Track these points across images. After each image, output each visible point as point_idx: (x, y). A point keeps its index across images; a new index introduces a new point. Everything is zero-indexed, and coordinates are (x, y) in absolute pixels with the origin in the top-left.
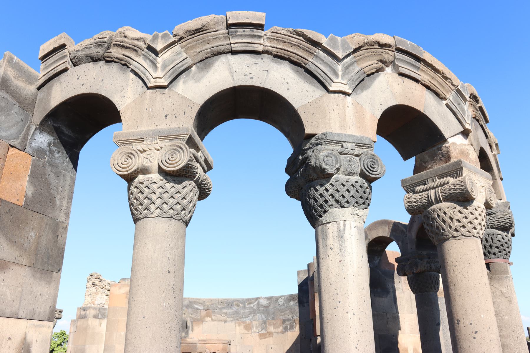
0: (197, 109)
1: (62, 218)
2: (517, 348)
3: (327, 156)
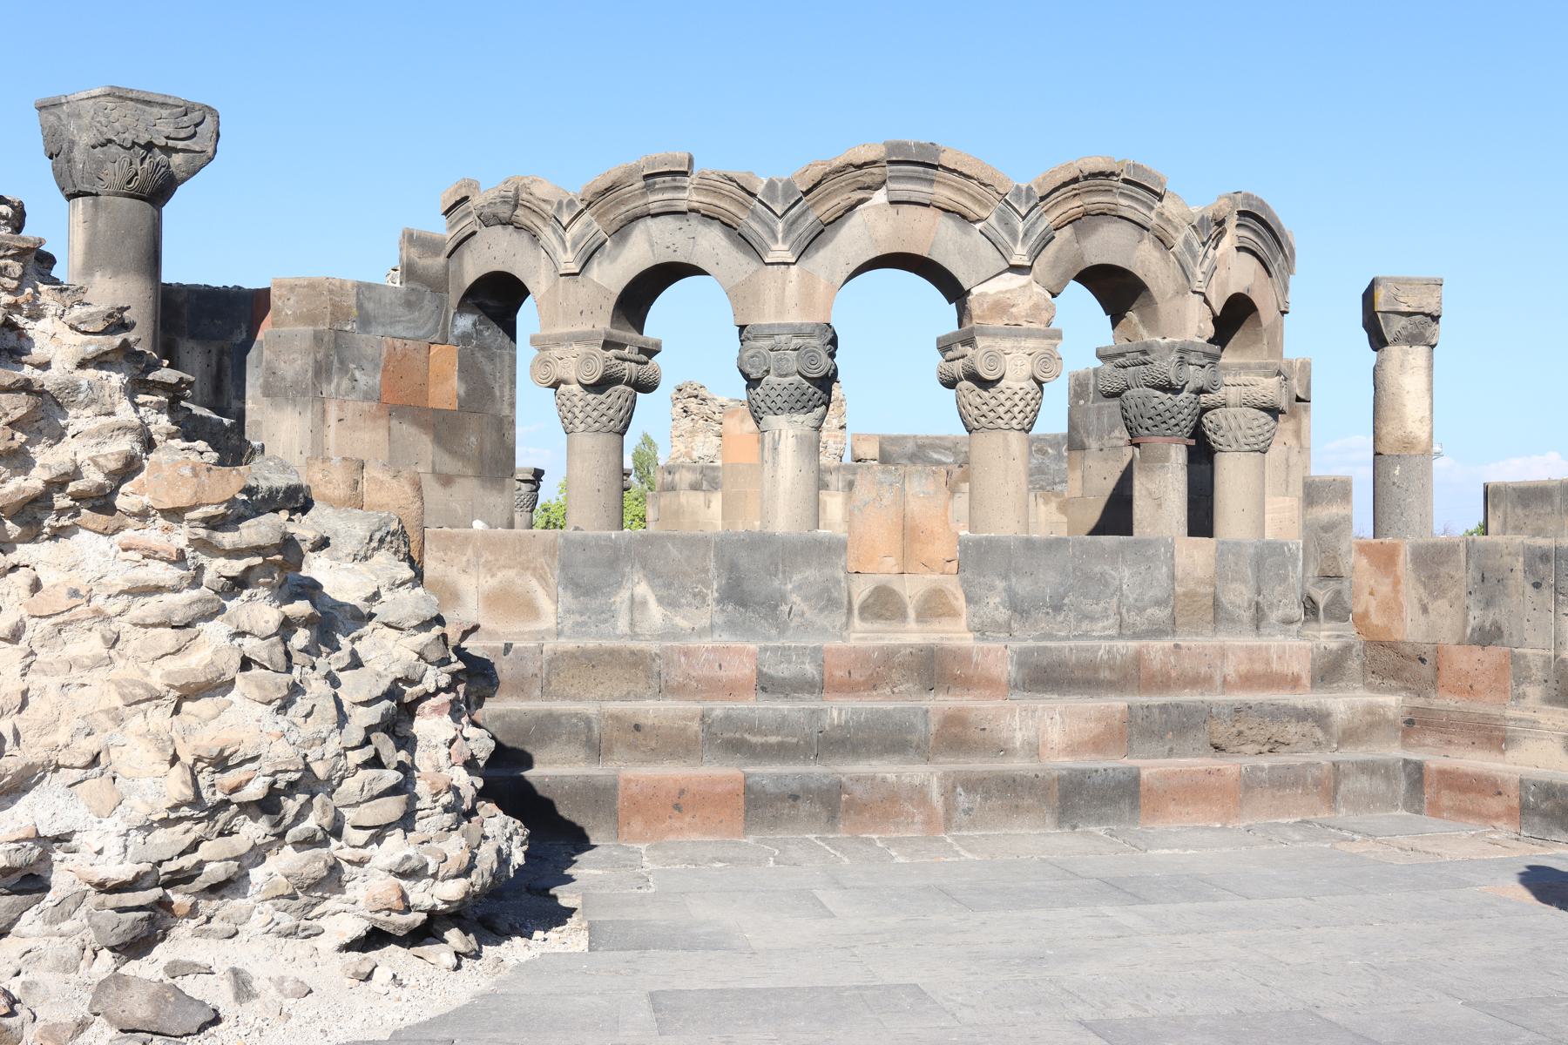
1: (506, 411)
3: (752, 357)
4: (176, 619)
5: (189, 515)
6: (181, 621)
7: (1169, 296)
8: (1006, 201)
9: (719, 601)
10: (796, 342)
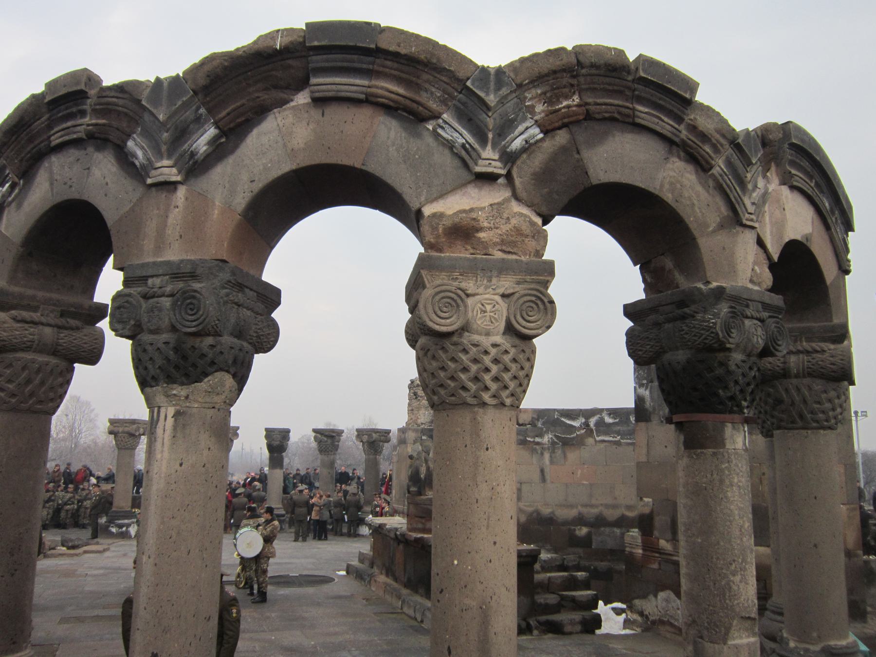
2: (709, 605)
7: (711, 229)
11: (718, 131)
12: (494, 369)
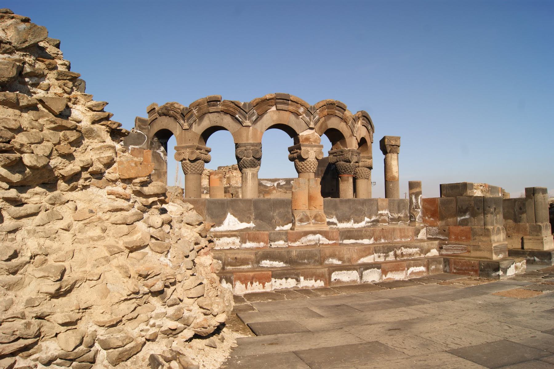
0: (199, 136)
4: (129, 221)
5: (134, 181)
6: (130, 222)
8: (308, 110)
9: (255, 219)
10: (252, 148)
11: (350, 116)
12: (313, 165)
